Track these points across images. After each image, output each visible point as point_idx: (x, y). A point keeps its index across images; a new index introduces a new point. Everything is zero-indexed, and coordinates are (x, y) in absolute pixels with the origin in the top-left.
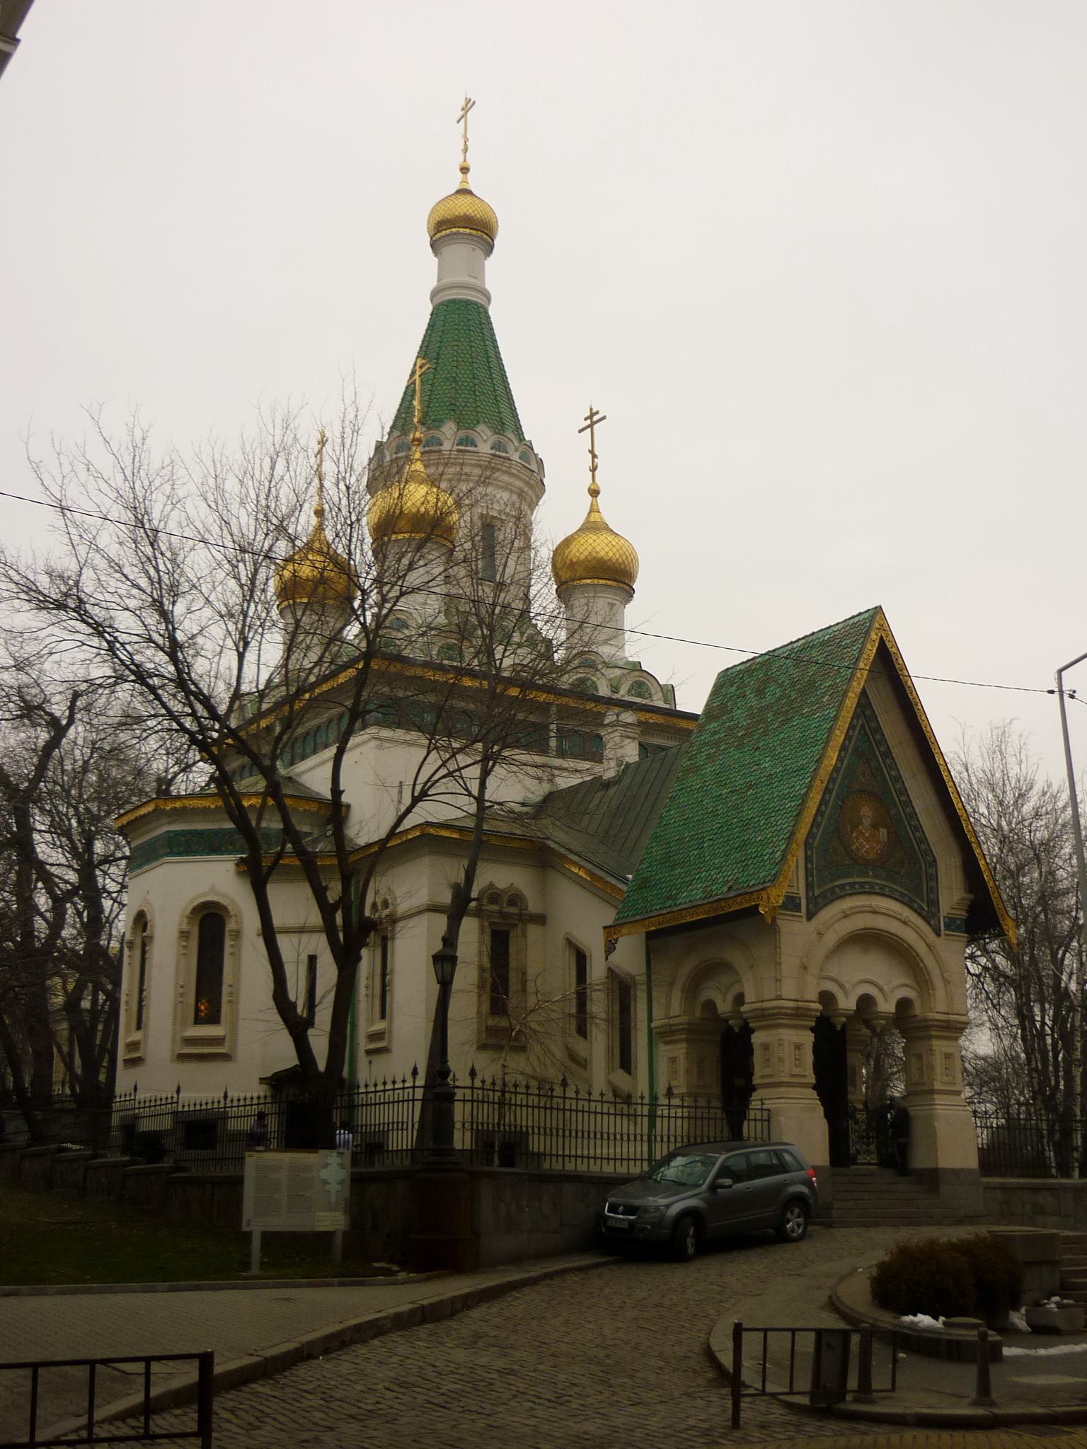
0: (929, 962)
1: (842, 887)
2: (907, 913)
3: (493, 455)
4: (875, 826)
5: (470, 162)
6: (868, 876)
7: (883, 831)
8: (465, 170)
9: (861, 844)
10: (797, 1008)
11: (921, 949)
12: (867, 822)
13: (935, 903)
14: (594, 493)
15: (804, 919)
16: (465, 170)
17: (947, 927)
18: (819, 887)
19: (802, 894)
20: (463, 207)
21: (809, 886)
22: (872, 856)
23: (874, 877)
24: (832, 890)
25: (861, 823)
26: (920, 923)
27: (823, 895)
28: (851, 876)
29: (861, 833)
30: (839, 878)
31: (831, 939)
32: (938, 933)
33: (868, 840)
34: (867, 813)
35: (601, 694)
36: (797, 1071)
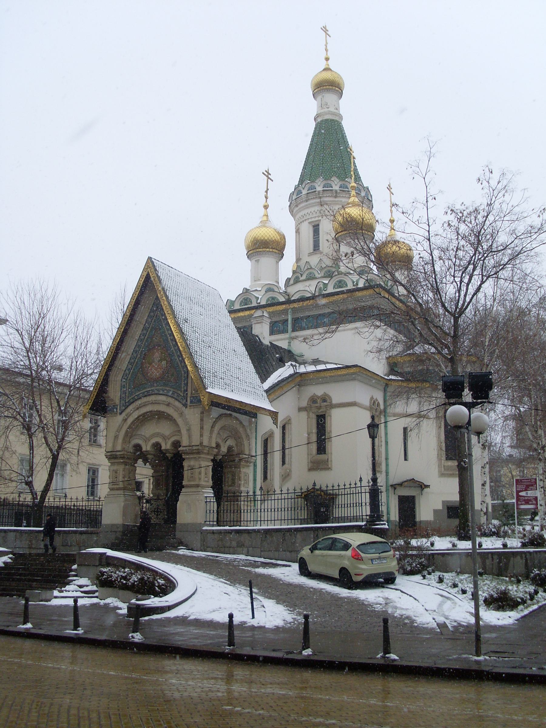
0: (179, 421)
3: (308, 193)
4: (161, 361)
5: (330, 55)
6: (154, 386)
7: (164, 363)
8: (327, 59)
10: (111, 455)
11: (175, 415)
12: (156, 361)
14: (266, 207)
15: (118, 414)
16: (327, 59)
17: (191, 402)
19: (117, 401)
20: (327, 75)
25: (154, 362)
26: (177, 404)
28: (145, 388)
32: (185, 405)
33: (156, 369)
34: (157, 355)
35: (281, 301)
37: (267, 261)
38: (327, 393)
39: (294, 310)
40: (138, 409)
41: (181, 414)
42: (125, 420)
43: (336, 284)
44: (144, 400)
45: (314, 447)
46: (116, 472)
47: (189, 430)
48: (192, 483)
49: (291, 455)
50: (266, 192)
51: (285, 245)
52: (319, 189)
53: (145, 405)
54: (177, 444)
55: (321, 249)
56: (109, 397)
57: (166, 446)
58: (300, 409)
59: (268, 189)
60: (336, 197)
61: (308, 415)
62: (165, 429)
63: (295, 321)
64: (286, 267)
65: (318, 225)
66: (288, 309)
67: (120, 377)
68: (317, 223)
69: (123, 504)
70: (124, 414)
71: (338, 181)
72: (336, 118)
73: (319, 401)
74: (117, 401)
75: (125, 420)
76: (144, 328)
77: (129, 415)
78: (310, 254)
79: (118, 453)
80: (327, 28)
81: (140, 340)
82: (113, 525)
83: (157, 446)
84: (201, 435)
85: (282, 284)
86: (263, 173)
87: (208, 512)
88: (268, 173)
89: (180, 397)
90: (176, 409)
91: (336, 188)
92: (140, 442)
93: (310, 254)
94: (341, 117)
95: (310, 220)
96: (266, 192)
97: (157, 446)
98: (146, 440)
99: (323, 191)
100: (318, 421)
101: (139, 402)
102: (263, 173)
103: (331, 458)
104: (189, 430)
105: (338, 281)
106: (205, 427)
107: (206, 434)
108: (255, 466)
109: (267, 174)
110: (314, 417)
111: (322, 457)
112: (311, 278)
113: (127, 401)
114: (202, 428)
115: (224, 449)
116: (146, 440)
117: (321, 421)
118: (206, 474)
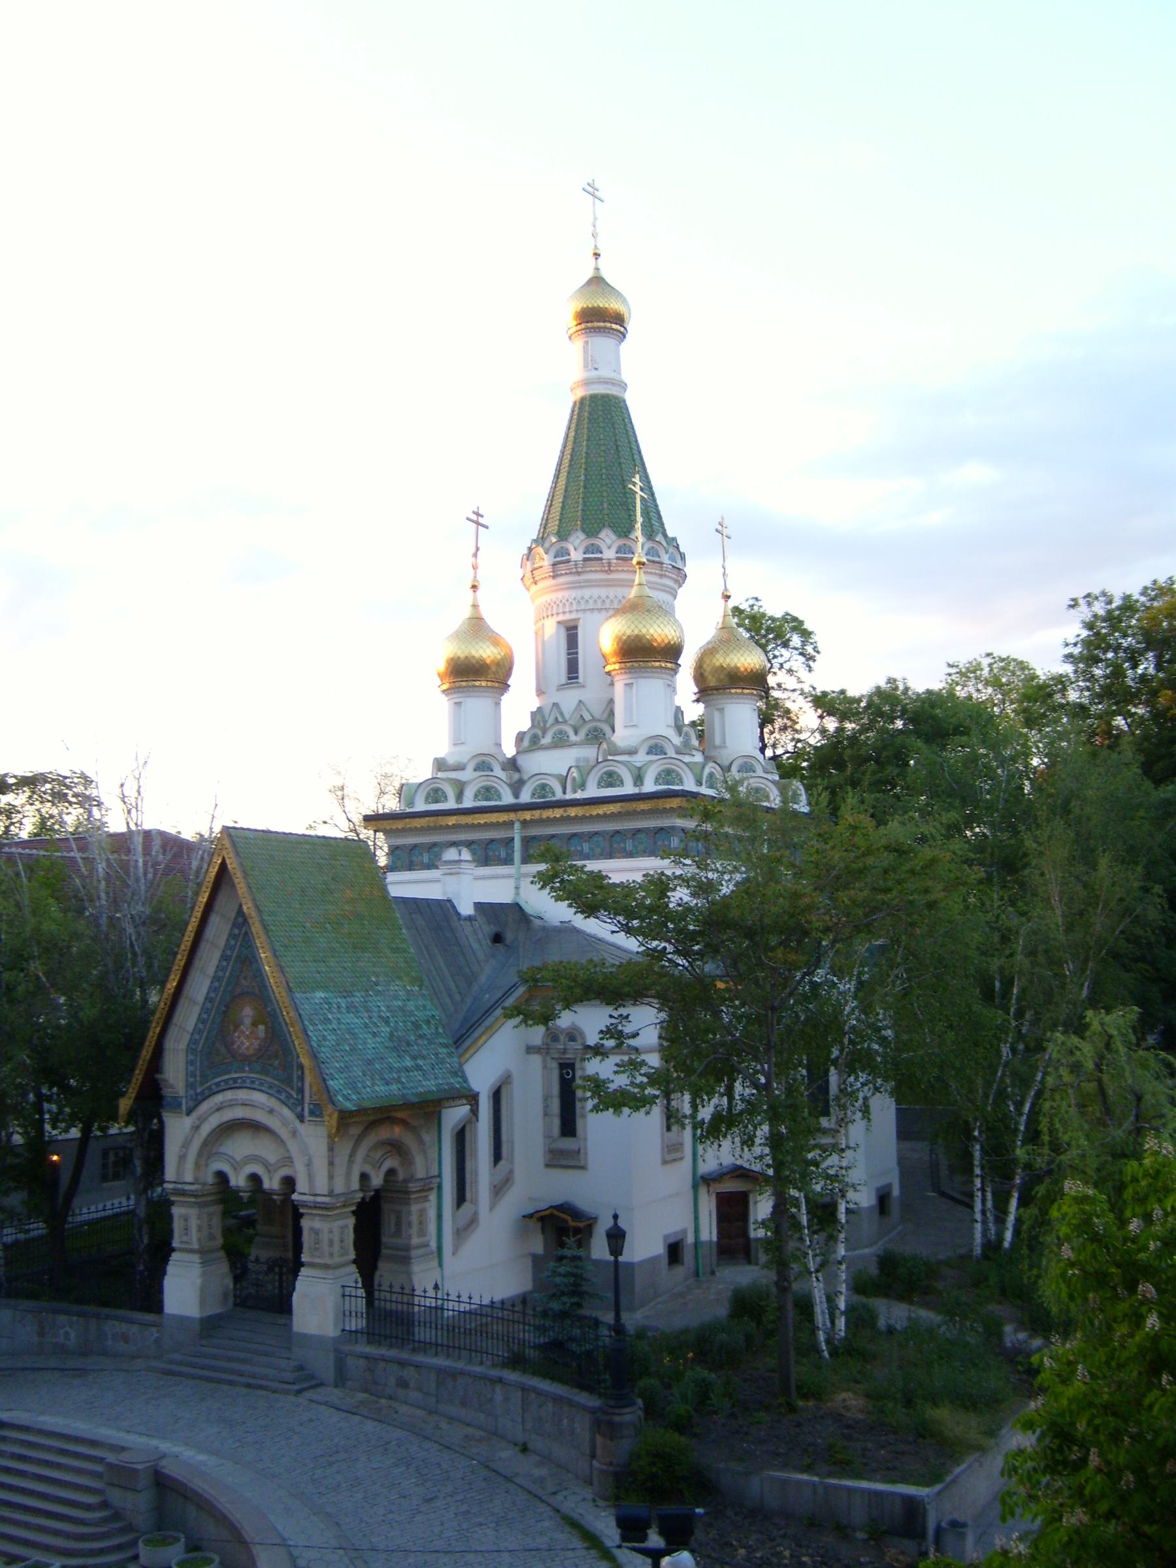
1: (218, 1084)
2: (273, 1103)
4: (254, 1024)
6: (244, 1071)
9: (242, 1043)
11: (283, 1132)
12: (248, 1021)
13: (301, 1091)
16: (597, 255)
17: (312, 1113)
18: (202, 1084)
19: (182, 1092)
21: (190, 1086)
22: (251, 1052)
23: (251, 1071)
24: (209, 1088)
25: (242, 1023)
26: (286, 1111)
27: (202, 1092)
28: (229, 1072)
29: (243, 1032)
30: (220, 1076)
31: (206, 1129)
32: (301, 1118)
33: (248, 1037)
36: (185, 1238)
37: (477, 705)
38: (578, 1023)
39: (525, 823)
40: (218, 1110)
41: (294, 1133)
42: (196, 1128)
43: (602, 777)
44: (229, 1095)
45: (557, 1122)
46: (186, 1220)
47: (309, 1165)
48: (317, 1260)
49: (512, 1142)
50: (475, 555)
51: (511, 669)
52: (576, 556)
53: (232, 1104)
54: (289, 1183)
55: (581, 680)
56: (165, 1080)
57: (271, 1183)
58: (530, 1050)
59: (478, 549)
60: (610, 571)
61: (544, 1061)
62: (266, 1150)
63: (527, 841)
64: (518, 708)
65: (576, 628)
66: (512, 823)
67: (183, 1045)
68: (572, 624)
69: (199, 1281)
70: (195, 1115)
71: (614, 537)
72: (613, 391)
73: (562, 1038)
74: (182, 1092)
75: (196, 1128)
76: (224, 957)
77: (202, 1120)
78: (561, 687)
79: (187, 1187)
80: (596, 186)
81: (216, 978)
82: (182, 1320)
83: (255, 1178)
84: (331, 1177)
85: (509, 750)
86: (468, 519)
87: (347, 1313)
88: (478, 514)
89: (292, 1101)
90: (285, 1123)
91: (609, 554)
92: (225, 1167)
93: (561, 687)
94: (623, 386)
95: (561, 618)
96: (475, 555)
97: (255, 1178)
98: (237, 1166)
99: (585, 560)
100: (562, 1077)
101: (219, 1098)
102: (468, 519)
103: (586, 1148)
104: (309, 1165)
105: (605, 773)
106: (337, 1161)
107: (340, 1171)
108: (440, 1187)
109: (477, 520)
110: (554, 1065)
111: (568, 1143)
112: (561, 742)
113: (199, 1090)
114: (331, 1163)
115: (377, 1181)
116: (237, 1166)
117: (568, 1074)
118: (342, 1241)
